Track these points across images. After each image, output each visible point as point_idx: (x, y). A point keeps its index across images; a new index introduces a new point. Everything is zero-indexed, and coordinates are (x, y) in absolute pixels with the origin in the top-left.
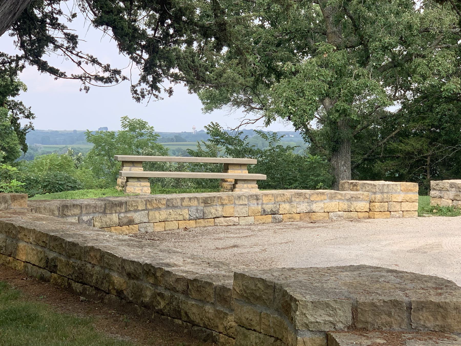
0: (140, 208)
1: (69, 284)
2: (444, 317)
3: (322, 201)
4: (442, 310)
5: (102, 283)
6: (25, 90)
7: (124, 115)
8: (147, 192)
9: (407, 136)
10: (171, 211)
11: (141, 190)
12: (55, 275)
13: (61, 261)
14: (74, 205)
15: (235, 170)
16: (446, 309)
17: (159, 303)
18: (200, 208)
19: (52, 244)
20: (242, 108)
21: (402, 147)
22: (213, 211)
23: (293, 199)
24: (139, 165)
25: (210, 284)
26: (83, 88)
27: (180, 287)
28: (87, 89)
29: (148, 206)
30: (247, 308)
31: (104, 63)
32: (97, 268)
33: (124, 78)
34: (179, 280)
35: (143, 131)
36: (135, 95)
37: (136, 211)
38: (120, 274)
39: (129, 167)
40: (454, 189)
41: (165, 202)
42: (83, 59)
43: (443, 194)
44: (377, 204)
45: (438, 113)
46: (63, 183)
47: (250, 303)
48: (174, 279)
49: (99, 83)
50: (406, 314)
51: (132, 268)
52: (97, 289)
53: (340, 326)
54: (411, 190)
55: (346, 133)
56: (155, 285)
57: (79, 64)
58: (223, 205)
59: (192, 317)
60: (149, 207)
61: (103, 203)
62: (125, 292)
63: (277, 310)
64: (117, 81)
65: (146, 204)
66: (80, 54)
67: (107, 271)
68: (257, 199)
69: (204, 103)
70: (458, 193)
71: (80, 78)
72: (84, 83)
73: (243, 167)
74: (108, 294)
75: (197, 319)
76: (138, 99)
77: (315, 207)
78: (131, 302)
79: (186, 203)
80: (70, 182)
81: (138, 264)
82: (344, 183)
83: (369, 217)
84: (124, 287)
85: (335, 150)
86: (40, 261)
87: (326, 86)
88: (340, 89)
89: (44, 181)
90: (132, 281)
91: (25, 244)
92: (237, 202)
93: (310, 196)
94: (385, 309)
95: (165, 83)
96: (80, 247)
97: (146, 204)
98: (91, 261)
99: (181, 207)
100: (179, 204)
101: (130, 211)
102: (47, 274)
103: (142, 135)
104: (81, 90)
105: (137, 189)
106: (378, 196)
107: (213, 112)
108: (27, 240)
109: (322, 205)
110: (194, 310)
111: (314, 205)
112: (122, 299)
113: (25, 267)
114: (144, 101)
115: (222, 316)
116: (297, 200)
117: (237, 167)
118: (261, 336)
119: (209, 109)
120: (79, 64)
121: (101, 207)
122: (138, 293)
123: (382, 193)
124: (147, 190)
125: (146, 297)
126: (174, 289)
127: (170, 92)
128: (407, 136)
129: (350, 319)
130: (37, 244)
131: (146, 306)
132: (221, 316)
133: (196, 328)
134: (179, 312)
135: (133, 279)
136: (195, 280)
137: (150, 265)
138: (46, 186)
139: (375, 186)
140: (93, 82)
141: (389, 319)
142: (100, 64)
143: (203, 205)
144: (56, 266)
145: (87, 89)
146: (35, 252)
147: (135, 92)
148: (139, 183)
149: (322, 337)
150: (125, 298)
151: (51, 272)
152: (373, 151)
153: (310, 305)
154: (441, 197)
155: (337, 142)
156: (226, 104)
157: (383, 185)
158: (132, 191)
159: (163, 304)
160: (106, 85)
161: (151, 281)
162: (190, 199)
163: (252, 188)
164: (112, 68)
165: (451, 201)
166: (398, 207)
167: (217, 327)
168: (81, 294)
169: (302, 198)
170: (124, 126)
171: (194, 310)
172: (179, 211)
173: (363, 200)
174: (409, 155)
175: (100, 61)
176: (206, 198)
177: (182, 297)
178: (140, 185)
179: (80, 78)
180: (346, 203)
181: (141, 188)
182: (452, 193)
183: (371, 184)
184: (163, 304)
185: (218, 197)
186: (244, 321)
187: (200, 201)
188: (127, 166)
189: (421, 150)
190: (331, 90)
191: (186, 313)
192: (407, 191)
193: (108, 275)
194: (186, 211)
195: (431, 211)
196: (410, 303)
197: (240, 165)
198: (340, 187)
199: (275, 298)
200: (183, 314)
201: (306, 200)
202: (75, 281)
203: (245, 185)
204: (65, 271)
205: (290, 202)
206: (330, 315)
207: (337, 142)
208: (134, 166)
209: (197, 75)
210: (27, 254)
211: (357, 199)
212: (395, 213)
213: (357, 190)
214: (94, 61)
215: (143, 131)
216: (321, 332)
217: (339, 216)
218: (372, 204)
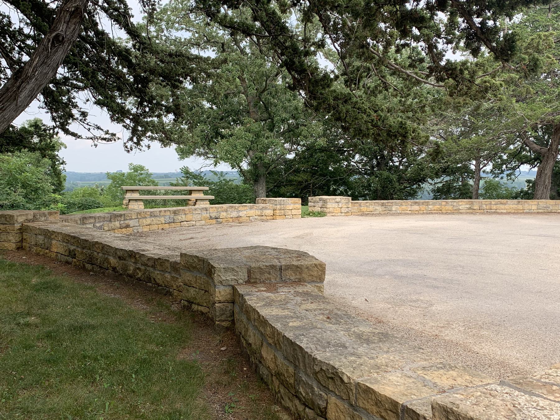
0: (133, 218)
1: (84, 265)
2: (300, 273)
3: (245, 210)
4: (299, 269)
5: (104, 263)
6: (66, 147)
7: (130, 163)
9: (299, 172)
10: (153, 218)
12: (75, 260)
13: (78, 251)
14: (90, 217)
16: (301, 269)
17: (138, 274)
18: (172, 216)
19: (72, 241)
20: (202, 157)
21: (296, 178)
22: (180, 218)
23: (228, 210)
24: (136, 192)
25: (168, 261)
26: (93, 145)
27: (150, 263)
28: (96, 146)
29: (138, 216)
30: (188, 274)
31: (105, 130)
32: (100, 255)
33: (119, 139)
34: (149, 259)
36: (126, 149)
37: (131, 219)
38: (114, 257)
40: (321, 201)
41: (149, 214)
42: (91, 127)
43: (316, 204)
44: (278, 211)
45: (316, 158)
46: (91, 204)
47: (190, 271)
48: (146, 259)
49: (104, 142)
50: (279, 273)
51: (121, 253)
52: (100, 267)
53: (241, 281)
54: (297, 203)
55: (262, 171)
56: (135, 263)
57: (89, 130)
58: (185, 214)
59: (157, 280)
60: (139, 217)
61: (109, 215)
62: (118, 268)
63: (205, 274)
64: (115, 140)
65: (137, 215)
66: (89, 124)
67: (106, 256)
68: (207, 210)
69: (179, 155)
70: (324, 204)
71: (91, 138)
72: (94, 142)
73: (200, 192)
74: (107, 270)
75: (160, 282)
76: (128, 151)
77: (241, 214)
78: (121, 274)
79: (162, 214)
81: (125, 250)
82: (258, 200)
83: (273, 219)
84: (116, 266)
85: (256, 181)
86: (65, 252)
87: (249, 143)
88: (257, 145)
89: (79, 204)
90: (122, 261)
91: (56, 241)
92: (194, 212)
93: (238, 207)
94: (267, 270)
95: (145, 142)
96: (90, 242)
97: (137, 215)
98: (96, 250)
99: (160, 216)
100: (158, 214)
101: (127, 219)
102: (70, 259)
103: (142, 174)
104: (92, 146)
105: (135, 206)
106: (278, 207)
107: (184, 160)
108: (57, 239)
109: (245, 212)
110: (159, 277)
111: (241, 213)
112: (116, 272)
113: (57, 255)
114: (132, 153)
115: (174, 279)
116: (231, 210)
117: (197, 192)
118: (197, 290)
119: (182, 158)
120: (89, 130)
121: (108, 217)
122: (125, 269)
123: (280, 205)
125: (130, 270)
126: (146, 265)
127: (149, 147)
128: (299, 172)
129: (246, 277)
130: (64, 242)
131: (130, 276)
132: (175, 279)
133: (160, 288)
134: (150, 278)
135: (122, 260)
136: (159, 259)
137: (132, 251)
138: (81, 206)
139: (276, 200)
140: (100, 141)
141: (269, 276)
142: (102, 130)
143: (173, 214)
144: (75, 255)
145: (96, 146)
146: (62, 246)
147: (126, 147)
148: (136, 203)
149: (230, 288)
150: (117, 272)
151: (72, 258)
152: (280, 181)
153: (222, 270)
154: (314, 206)
155: (257, 176)
156: (192, 155)
157: (281, 200)
159: (140, 274)
160: (108, 143)
161: (133, 261)
162: (165, 211)
163: (206, 204)
164: (110, 132)
165: (320, 208)
166: (290, 213)
167: (173, 286)
168: (90, 271)
169: (233, 209)
170: (131, 169)
171: (159, 277)
172: (158, 219)
173: (269, 209)
174: (300, 183)
175: (102, 128)
176: (175, 210)
177: (151, 269)
179: (91, 138)
180: (260, 211)
182: (320, 204)
183: (274, 200)
184: (140, 274)
185: (183, 210)
186: (187, 281)
187: (172, 212)
189: (307, 180)
190: (252, 146)
191: (154, 279)
192: (295, 203)
193: (107, 258)
194: (163, 218)
195: (309, 214)
196: (281, 266)
197: (199, 191)
198: (256, 202)
199: (204, 267)
200: (152, 279)
201: (236, 210)
202: (87, 263)
203: (202, 203)
204: (81, 257)
205: (226, 211)
206: (234, 276)
207: (257, 176)
208: (133, 193)
209: (166, 136)
210: (57, 248)
211: (266, 208)
212: (288, 216)
213: (266, 203)
214: (98, 128)
216: (229, 285)
217: (256, 219)
218: (275, 211)
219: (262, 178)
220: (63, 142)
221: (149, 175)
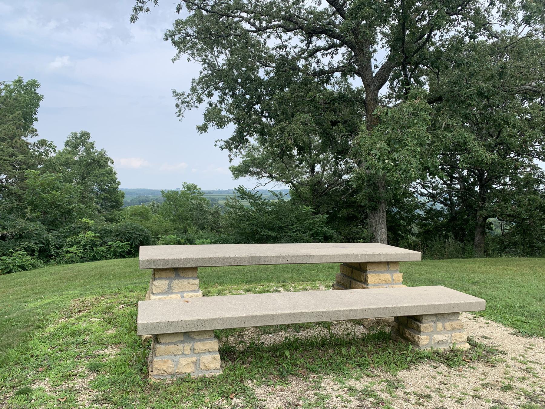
8: (212, 366)
11: (195, 363)
15: (378, 272)
20: (255, 177)
24: (190, 274)
39: (166, 278)
69: (234, 174)
73: (392, 267)
80: (138, 231)
103: (194, 193)
105: (184, 361)
117: (382, 268)
124: (211, 362)
138: (118, 235)
158: (170, 370)
181: (194, 359)
203: (440, 325)
208: (178, 277)
219: (383, 204)
221: (202, 193)
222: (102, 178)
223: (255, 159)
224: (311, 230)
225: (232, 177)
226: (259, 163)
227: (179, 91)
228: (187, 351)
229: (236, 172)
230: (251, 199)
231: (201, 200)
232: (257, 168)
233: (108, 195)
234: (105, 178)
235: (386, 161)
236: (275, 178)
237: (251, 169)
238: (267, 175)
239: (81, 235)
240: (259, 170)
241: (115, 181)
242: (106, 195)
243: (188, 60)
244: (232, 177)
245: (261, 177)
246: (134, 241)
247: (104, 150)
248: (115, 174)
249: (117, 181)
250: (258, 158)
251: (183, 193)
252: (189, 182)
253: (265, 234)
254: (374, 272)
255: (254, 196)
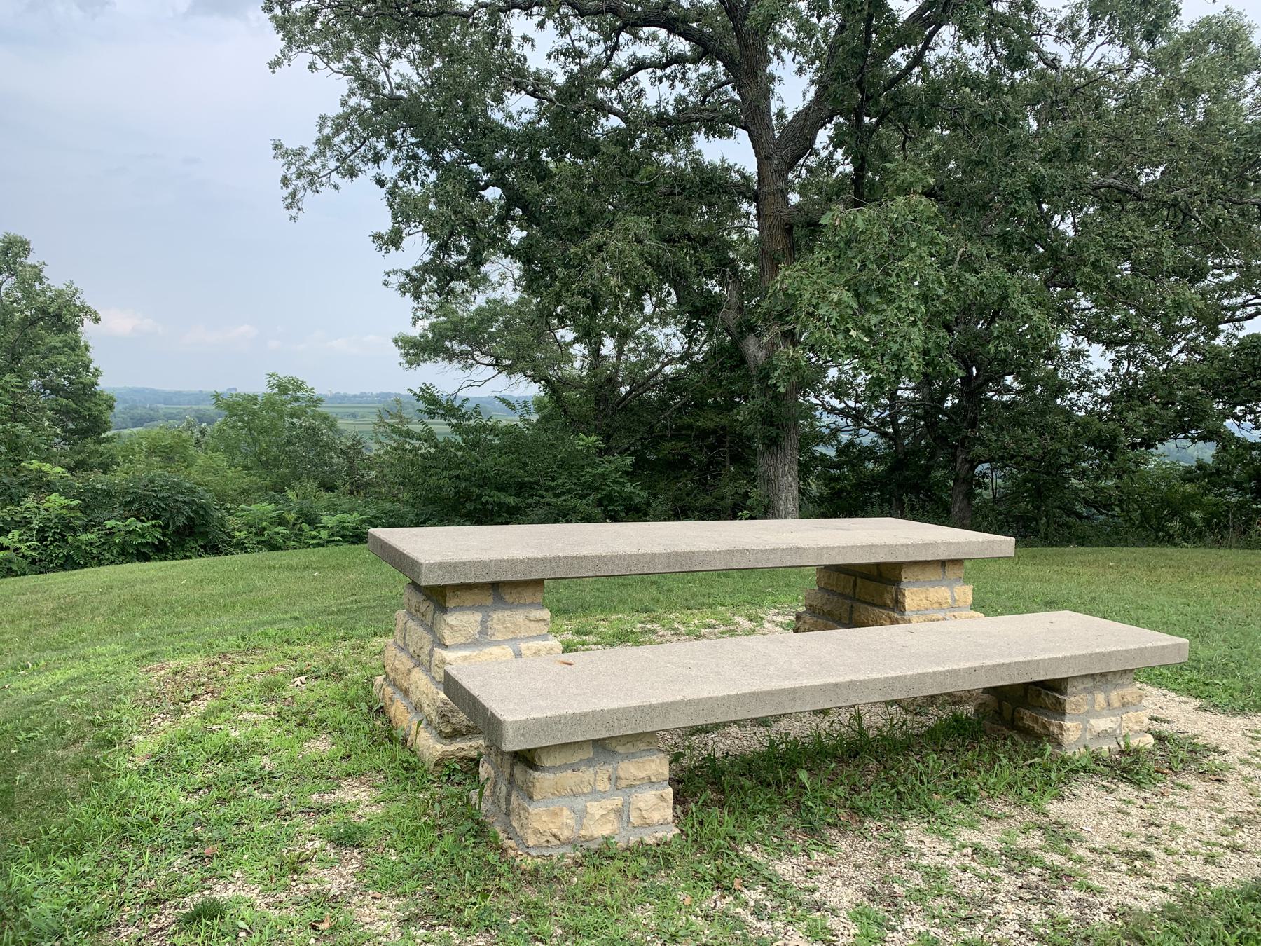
6: (97, 320)
8: (656, 817)
24: (528, 595)
35: (299, 394)
39: (473, 608)
46: (166, 495)
73: (951, 573)
80: (182, 493)
89: (127, 493)
103: (297, 399)
105: (596, 809)
117: (931, 574)
124: (655, 808)
138: (131, 503)
158: (566, 834)
178: (615, 780)
181: (618, 801)
188: (461, 608)
203: (1100, 697)
215: (299, 394)
220: (87, 304)
221: (316, 401)
222: (52, 359)
223: (462, 320)
224: (596, 489)
225: (400, 364)
226: (471, 331)
227: (290, 145)
228: (604, 785)
229: (411, 351)
230: (453, 416)
231: (314, 417)
232: (461, 343)
233: (70, 402)
234: (63, 358)
235: (853, 333)
236: (507, 367)
237: (448, 344)
238: (487, 360)
239: (30, 503)
240: (465, 347)
241: (87, 368)
242: (65, 401)
243: (310, 67)
244: (400, 364)
245: (471, 366)
246: (172, 517)
247: (74, 286)
248: (87, 348)
249: (92, 366)
250: (471, 320)
251: (270, 403)
252: (285, 373)
253: (491, 500)
254: (916, 582)
255: (459, 409)
